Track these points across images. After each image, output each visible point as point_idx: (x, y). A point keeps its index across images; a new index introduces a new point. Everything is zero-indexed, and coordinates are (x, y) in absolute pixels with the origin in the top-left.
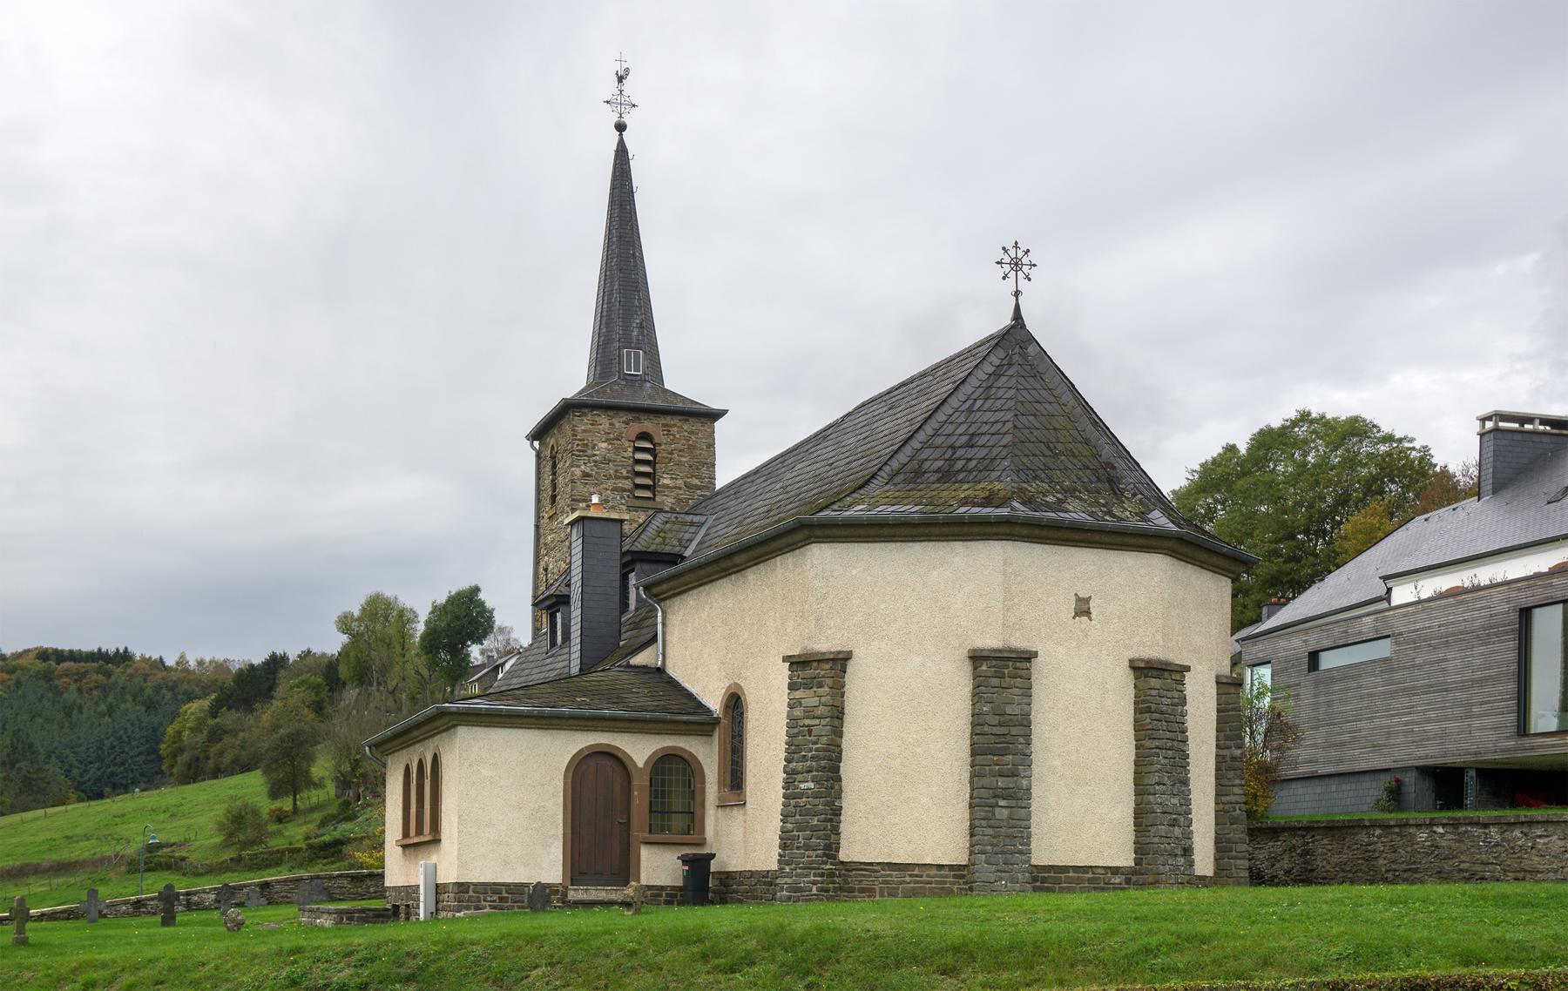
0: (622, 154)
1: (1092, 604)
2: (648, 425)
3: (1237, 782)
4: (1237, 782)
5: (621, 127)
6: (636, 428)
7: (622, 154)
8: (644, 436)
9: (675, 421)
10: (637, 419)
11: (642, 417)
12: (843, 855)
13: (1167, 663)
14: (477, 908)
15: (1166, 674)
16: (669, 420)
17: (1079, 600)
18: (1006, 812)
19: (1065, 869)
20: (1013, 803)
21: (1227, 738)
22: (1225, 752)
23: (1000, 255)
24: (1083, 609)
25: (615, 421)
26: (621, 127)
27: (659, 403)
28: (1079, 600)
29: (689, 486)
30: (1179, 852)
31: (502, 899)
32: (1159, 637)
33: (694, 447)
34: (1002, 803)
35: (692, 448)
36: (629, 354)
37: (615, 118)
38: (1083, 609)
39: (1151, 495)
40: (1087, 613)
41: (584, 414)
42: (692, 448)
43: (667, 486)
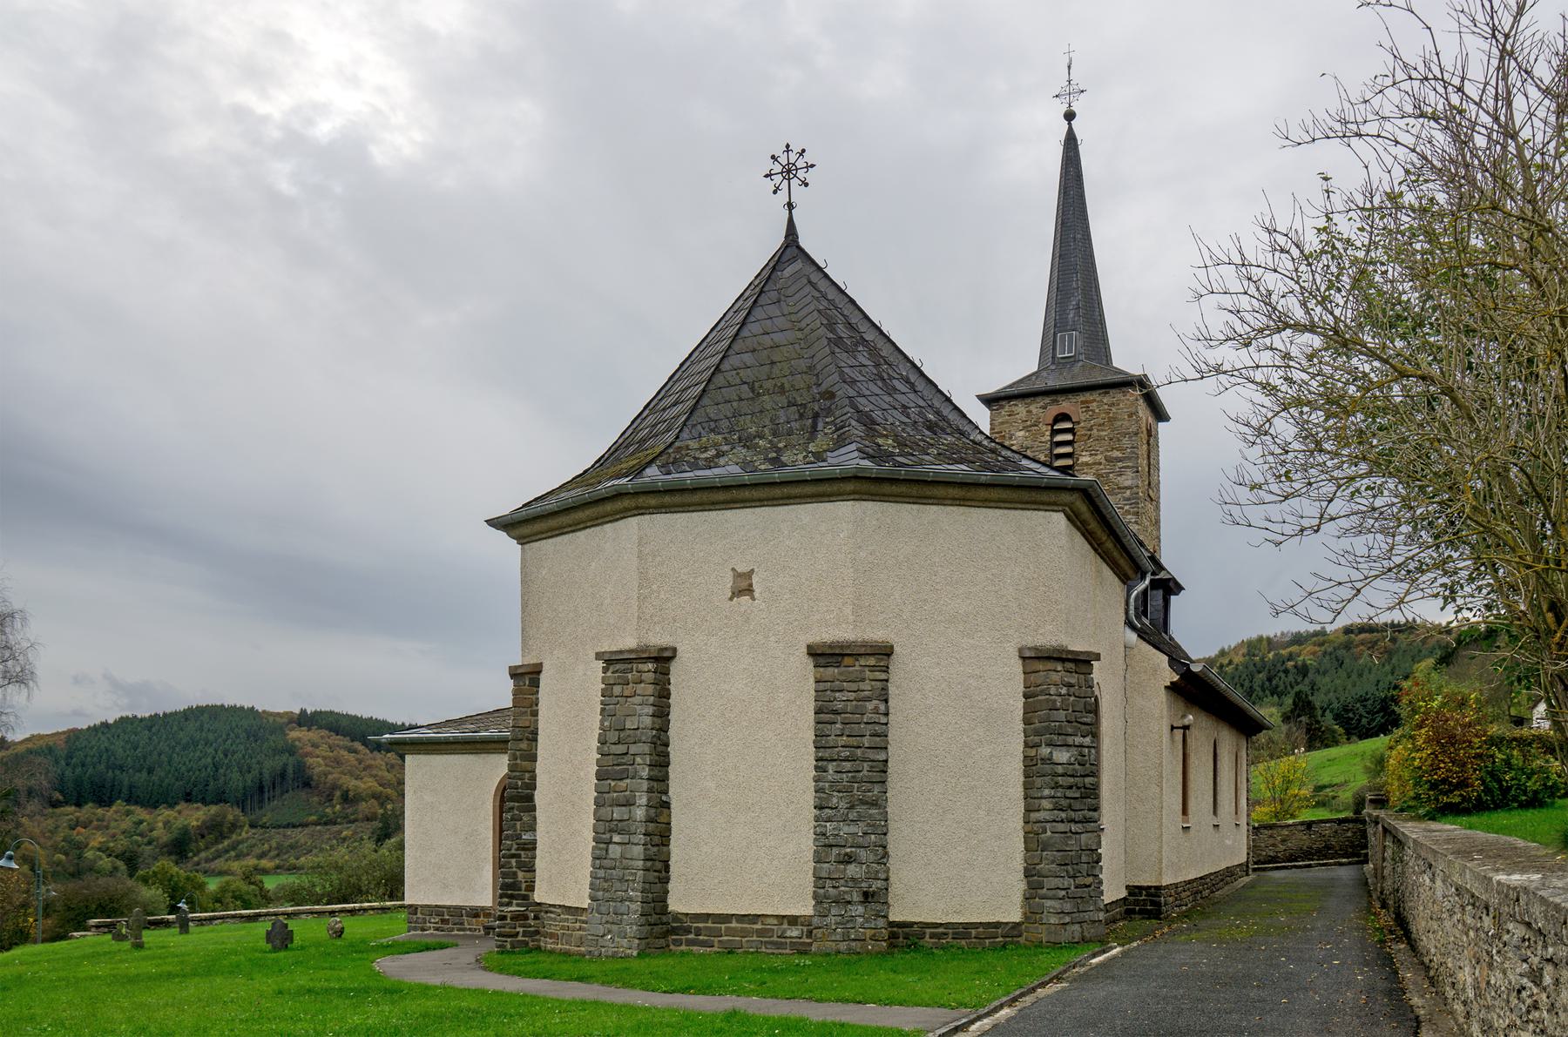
0: (1071, 142)
1: (755, 580)
2: (1065, 405)
3: (1047, 792)
4: (1047, 792)
5: (1070, 116)
6: (1054, 410)
7: (1071, 142)
8: (1064, 417)
9: (1095, 395)
10: (1055, 402)
11: (1060, 398)
12: (539, 896)
13: (850, 645)
14: (423, 930)
15: (847, 661)
16: (1088, 396)
17: (738, 576)
18: (618, 849)
19: (726, 918)
20: (626, 838)
21: (1037, 733)
22: (1032, 752)
23: (769, 165)
24: (743, 587)
25: (1032, 408)
26: (1070, 116)
27: (1110, 378)
28: (738, 576)
29: (1109, 460)
30: (856, 897)
31: (443, 921)
32: (848, 610)
33: (1115, 419)
34: (616, 838)
35: (1112, 420)
36: (1063, 338)
37: (1064, 108)
38: (743, 587)
39: (940, 415)
40: (749, 590)
41: (1002, 407)
42: (1112, 420)
43: (1087, 464)
